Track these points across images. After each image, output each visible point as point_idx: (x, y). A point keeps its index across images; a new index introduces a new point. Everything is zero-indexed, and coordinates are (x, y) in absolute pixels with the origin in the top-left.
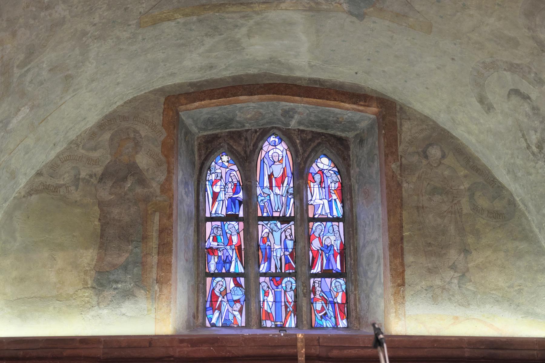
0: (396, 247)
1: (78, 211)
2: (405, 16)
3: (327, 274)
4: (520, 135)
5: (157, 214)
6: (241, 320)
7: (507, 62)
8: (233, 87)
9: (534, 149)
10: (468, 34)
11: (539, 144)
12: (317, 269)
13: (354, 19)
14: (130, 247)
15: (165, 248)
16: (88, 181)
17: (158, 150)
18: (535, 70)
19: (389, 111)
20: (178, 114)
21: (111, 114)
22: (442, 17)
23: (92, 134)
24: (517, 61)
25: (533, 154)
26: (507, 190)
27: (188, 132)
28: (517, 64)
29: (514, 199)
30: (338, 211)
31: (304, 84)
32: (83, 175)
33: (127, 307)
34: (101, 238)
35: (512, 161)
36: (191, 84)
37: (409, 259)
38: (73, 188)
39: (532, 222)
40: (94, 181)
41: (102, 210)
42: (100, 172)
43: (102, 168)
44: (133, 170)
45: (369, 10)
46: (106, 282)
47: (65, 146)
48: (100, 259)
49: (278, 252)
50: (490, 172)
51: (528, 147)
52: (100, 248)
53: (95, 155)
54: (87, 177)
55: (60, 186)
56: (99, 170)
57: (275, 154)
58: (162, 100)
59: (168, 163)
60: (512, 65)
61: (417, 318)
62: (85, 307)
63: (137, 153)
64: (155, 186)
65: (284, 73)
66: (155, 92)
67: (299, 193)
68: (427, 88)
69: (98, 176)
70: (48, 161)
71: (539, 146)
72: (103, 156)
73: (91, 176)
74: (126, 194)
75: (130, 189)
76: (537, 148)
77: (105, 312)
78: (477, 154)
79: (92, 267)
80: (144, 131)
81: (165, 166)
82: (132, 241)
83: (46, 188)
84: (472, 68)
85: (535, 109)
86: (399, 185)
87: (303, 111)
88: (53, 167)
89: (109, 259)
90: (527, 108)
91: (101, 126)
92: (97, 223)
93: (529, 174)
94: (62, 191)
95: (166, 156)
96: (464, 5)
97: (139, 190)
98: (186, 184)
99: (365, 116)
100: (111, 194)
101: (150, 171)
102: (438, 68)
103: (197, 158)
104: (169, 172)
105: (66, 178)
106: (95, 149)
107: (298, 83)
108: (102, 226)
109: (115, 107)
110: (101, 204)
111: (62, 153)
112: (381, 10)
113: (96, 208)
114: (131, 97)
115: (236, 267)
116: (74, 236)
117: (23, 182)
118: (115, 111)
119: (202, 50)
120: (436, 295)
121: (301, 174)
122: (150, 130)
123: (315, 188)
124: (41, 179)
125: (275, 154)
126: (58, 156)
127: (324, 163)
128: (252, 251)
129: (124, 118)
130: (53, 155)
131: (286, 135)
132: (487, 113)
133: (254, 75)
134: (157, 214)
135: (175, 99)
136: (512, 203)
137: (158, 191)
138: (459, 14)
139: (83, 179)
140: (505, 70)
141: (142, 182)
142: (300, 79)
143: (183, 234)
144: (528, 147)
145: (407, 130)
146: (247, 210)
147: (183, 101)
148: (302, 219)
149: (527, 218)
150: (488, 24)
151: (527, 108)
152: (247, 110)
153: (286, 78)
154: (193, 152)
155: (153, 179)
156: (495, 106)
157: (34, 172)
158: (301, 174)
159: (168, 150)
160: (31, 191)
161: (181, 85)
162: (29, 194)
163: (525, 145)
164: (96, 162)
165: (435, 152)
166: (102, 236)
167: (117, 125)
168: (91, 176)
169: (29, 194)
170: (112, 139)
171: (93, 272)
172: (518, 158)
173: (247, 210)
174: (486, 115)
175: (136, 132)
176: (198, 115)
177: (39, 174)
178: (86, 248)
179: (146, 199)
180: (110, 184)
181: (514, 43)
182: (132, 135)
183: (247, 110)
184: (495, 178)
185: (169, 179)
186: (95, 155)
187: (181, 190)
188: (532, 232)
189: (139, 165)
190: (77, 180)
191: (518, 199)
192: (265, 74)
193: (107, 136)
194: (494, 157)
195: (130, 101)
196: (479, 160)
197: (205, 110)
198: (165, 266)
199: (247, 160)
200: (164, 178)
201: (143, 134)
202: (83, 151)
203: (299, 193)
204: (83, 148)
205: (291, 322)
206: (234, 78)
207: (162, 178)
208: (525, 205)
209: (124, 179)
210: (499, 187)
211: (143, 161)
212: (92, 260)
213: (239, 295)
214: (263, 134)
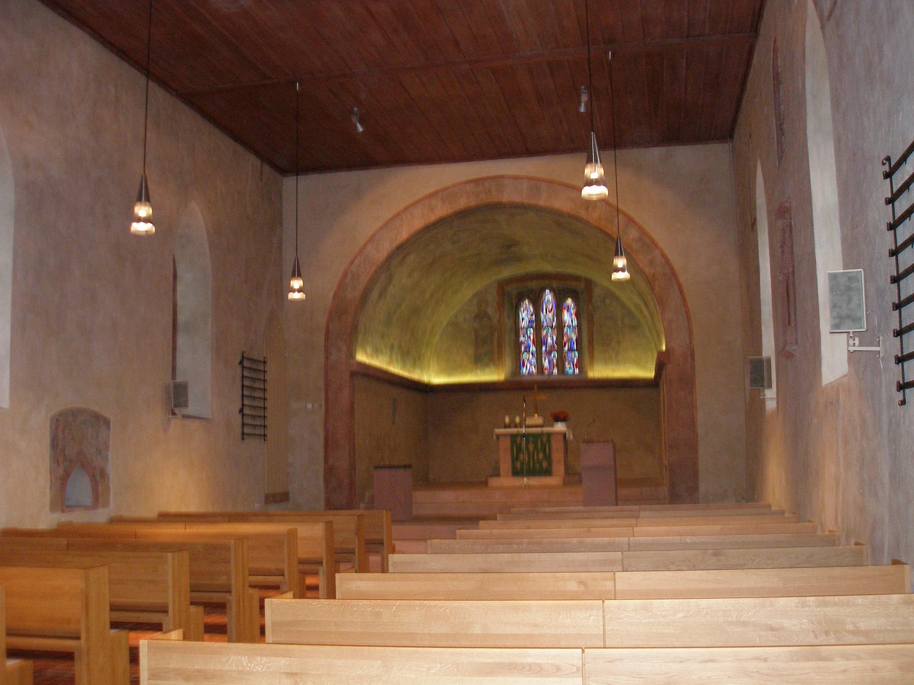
0: (591, 343)
3: (571, 350)
6: (534, 370)
12: (566, 348)
15: (500, 346)
19: (589, 283)
30: (575, 323)
33: (487, 370)
37: (596, 347)
44: (486, 314)
46: (479, 360)
49: (549, 340)
57: (548, 296)
61: (599, 371)
62: (471, 371)
64: (495, 321)
67: (559, 315)
77: (479, 372)
83: (453, 324)
86: (592, 316)
87: (555, 284)
98: (509, 317)
99: (582, 285)
115: (533, 348)
120: (607, 361)
121: (559, 308)
122: (492, 298)
123: (565, 312)
125: (548, 296)
127: (569, 301)
128: (539, 341)
131: (552, 290)
141: (489, 319)
143: (508, 339)
145: (597, 292)
146: (538, 325)
148: (560, 325)
152: (533, 285)
158: (559, 308)
159: (500, 306)
165: (608, 301)
167: (480, 298)
173: (538, 325)
176: (513, 289)
183: (533, 285)
187: (506, 320)
198: (500, 352)
199: (537, 304)
203: (559, 315)
205: (555, 371)
211: (490, 311)
213: (534, 361)
214: (542, 290)
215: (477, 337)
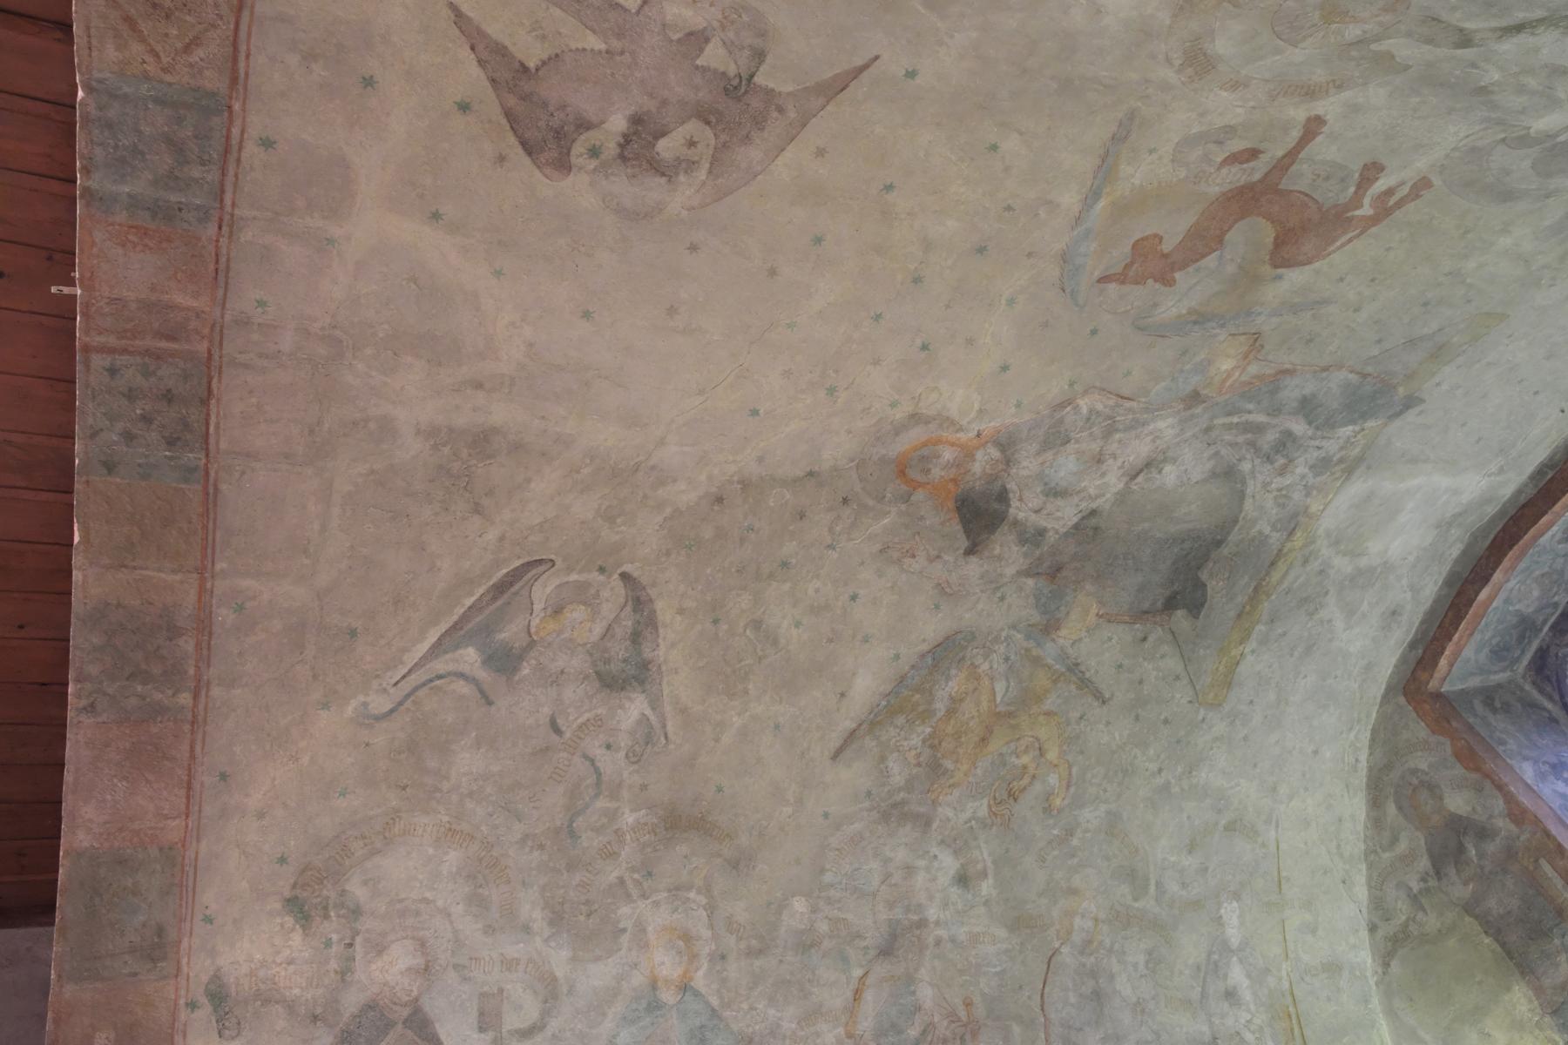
1: (1452, 942)
5: (1543, 862)
8: (1459, 594)
14: (1557, 942)
16: (1428, 890)
17: (1459, 770)
20: (1438, 696)
21: (1369, 777)
23: (1376, 822)
27: (1489, 696)
31: (1531, 492)
32: (1416, 886)
34: (1511, 958)
36: (1413, 645)
38: (1420, 915)
40: (1433, 883)
41: (1476, 917)
42: (1429, 864)
43: (1426, 856)
47: (1364, 867)
48: (1539, 991)
52: (1522, 973)
53: (1403, 846)
54: (1422, 885)
55: (1406, 925)
56: (1424, 863)
58: (1402, 700)
59: (1487, 776)
63: (1441, 799)
64: (1503, 824)
65: (1491, 510)
66: (1386, 697)
69: (1432, 872)
70: (1365, 903)
72: (1411, 840)
73: (1423, 880)
74: (1482, 868)
75: (1481, 856)
79: (1539, 1010)
80: (1421, 762)
81: (1488, 784)
82: (1551, 930)
88: (1378, 904)
89: (1547, 982)
91: (1375, 803)
92: (1487, 941)
94: (1412, 928)
95: (1478, 769)
97: (1491, 847)
100: (1466, 883)
101: (1479, 809)
103: (1549, 705)
104: (1500, 787)
105: (1403, 909)
106: (1394, 840)
107: (1523, 499)
108: (1497, 940)
109: (1363, 764)
110: (1468, 908)
111: (1369, 878)
113: (1468, 919)
114: (1368, 734)
116: (1480, 983)
117: (1365, 958)
118: (1370, 769)
119: (1339, 624)
122: (1428, 755)
124: (1380, 933)
126: (1370, 887)
129: (1388, 767)
130: (1362, 892)
133: (1464, 553)
134: (1543, 862)
135: (1415, 683)
137: (1512, 827)
139: (1420, 891)
142: (1519, 492)
147: (1424, 676)
153: (1502, 512)
154: (1534, 705)
155: (1491, 817)
157: (1364, 934)
160: (1385, 960)
161: (1403, 660)
162: (1386, 965)
164: (1408, 859)
166: (1509, 954)
168: (1423, 880)
169: (1386, 965)
170: (1400, 808)
171: (1547, 1019)
175: (1414, 772)
177: (1373, 929)
178: (1509, 989)
179: (1510, 853)
180: (1452, 871)
182: (1415, 781)
185: (1509, 798)
186: (1403, 846)
189: (1459, 812)
190: (1414, 899)
192: (1475, 538)
193: (1391, 809)
195: (1373, 740)
197: (1468, 652)
200: (1501, 802)
201: (1424, 766)
202: (1387, 855)
204: (1384, 851)
206: (1448, 582)
207: (1499, 804)
209: (1461, 849)
211: (1458, 803)
212: (1530, 1001)
215: (1494, 928)
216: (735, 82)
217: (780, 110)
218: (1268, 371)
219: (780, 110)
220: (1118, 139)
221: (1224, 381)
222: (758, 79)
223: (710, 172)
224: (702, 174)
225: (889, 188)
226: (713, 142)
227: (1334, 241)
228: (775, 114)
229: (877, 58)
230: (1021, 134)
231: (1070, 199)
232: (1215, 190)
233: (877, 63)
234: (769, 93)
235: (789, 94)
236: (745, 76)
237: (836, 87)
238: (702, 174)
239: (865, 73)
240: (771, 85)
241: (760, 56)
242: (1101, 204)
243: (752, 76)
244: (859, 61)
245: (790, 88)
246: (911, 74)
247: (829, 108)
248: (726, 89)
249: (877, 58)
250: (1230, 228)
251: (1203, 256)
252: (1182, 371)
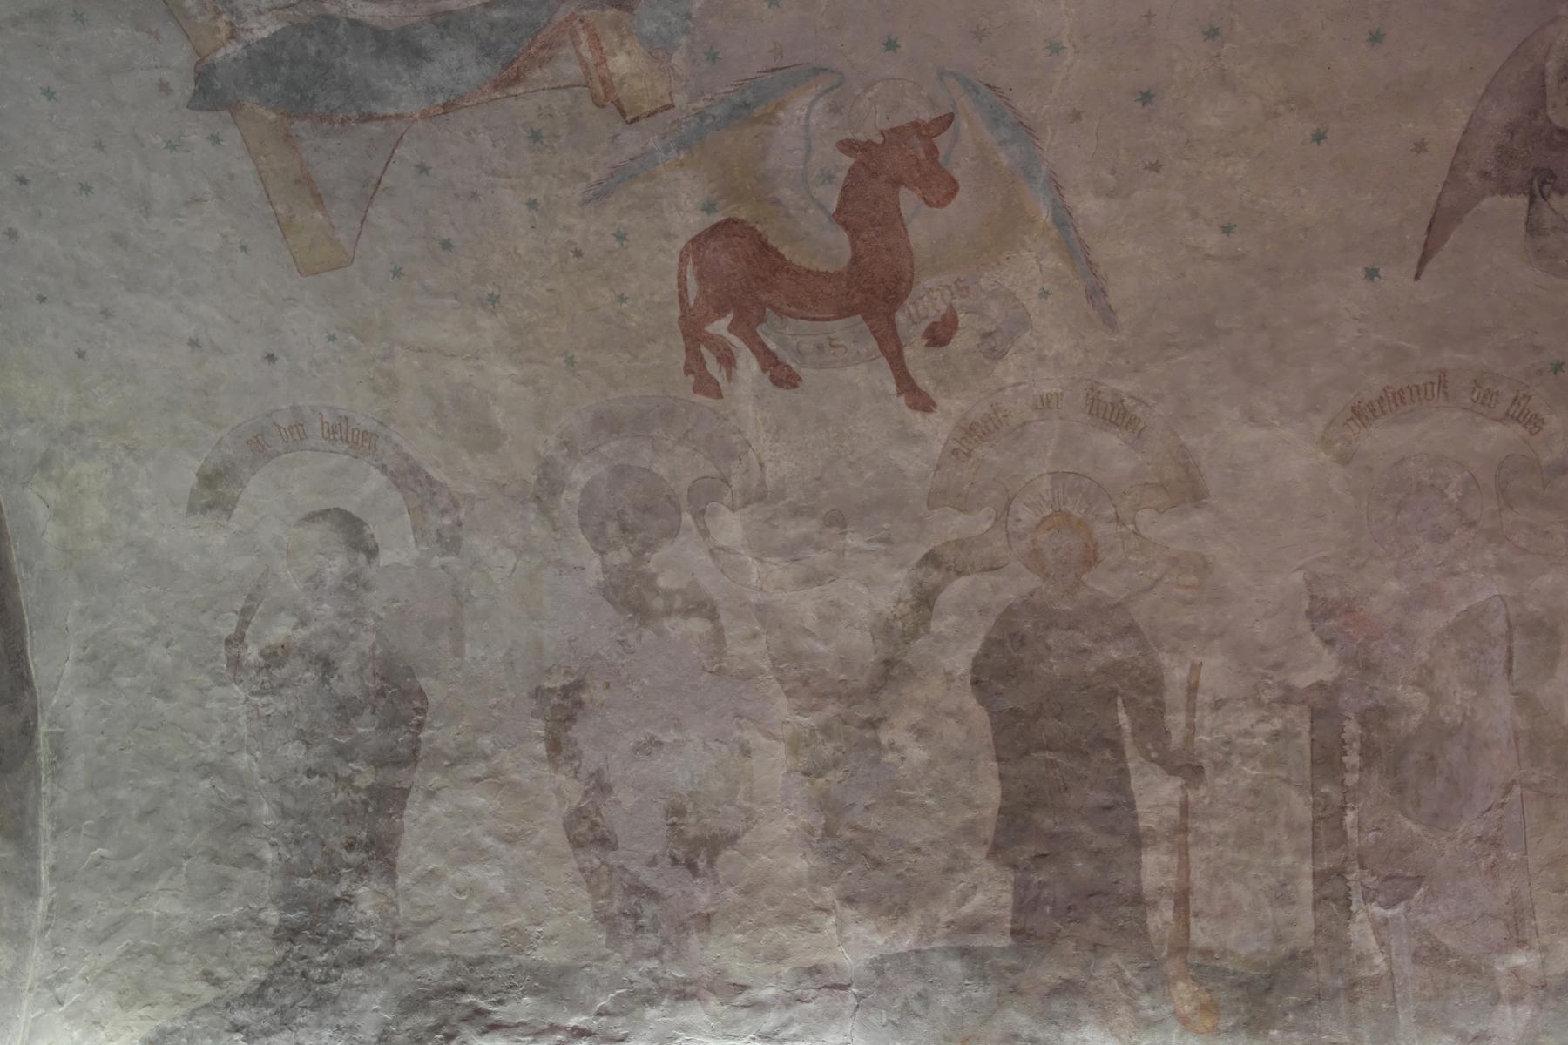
2: (319, 200)
4: (239, 605)
7: (407, 458)
9: (252, 653)
10: (397, 348)
11: (279, 651)
13: (183, 88)
18: (462, 515)
22: (397, 273)
24: (437, 474)
25: (235, 663)
26: (33, 695)
28: (428, 477)
29: (35, 726)
35: (135, 643)
39: (44, 802)
45: (260, 110)
50: (22, 630)
51: (237, 640)
60: (415, 470)
68: (81, 355)
71: (275, 654)
76: (262, 654)
78: (18, 570)
84: (294, 408)
85: (354, 584)
90: (336, 566)
93: (164, 694)
96: (493, 299)
102: (194, 343)
112: (289, 139)
132: (191, 509)
136: (28, 731)
138: (450, 301)
140: (383, 468)
144: (237, 640)
149: (38, 787)
150: (480, 368)
151: (336, 566)
156: (239, 510)
163: (227, 631)
172: (167, 646)
174: (183, 509)
181: (487, 438)
184: (23, 651)
188: (35, 825)
191: (43, 728)
194: (77, 604)
196: (16, 586)
208: (58, 753)
210: (21, 676)
216: (1546, 188)
217: (1485, 175)
218: (537, 73)
219: (1485, 175)
220: (1096, 293)
221: (595, 39)
222: (1522, 201)
223: (1543, 74)
224: (1552, 66)
225: (1319, 137)
226: (1550, 112)
227: (700, 277)
228: (1489, 168)
229: (1417, 277)
230: (1208, 256)
231: (1089, 207)
232: (926, 282)
233: (1414, 271)
234: (1506, 190)
235: (1484, 196)
236: (1540, 200)
237: (1439, 225)
238: (1552, 66)
239: (1418, 255)
240: (1507, 199)
241: (1533, 228)
242: (1045, 215)
243: (1531, 202)
244: (1432, 266)
245: (1487, 203)
246: (1371, 274)
247: (1434, 198)
248: (1554, 176)
249: (1417, 277)
250: (854, 247)
251: (844, 200)
252: (686, 31)
